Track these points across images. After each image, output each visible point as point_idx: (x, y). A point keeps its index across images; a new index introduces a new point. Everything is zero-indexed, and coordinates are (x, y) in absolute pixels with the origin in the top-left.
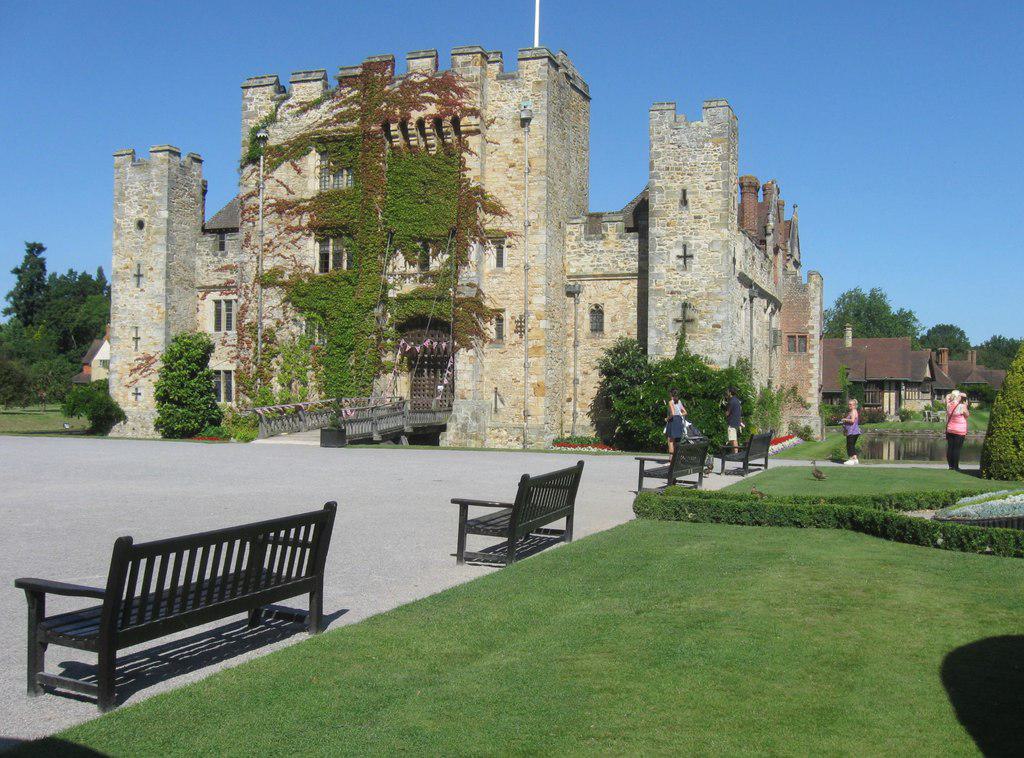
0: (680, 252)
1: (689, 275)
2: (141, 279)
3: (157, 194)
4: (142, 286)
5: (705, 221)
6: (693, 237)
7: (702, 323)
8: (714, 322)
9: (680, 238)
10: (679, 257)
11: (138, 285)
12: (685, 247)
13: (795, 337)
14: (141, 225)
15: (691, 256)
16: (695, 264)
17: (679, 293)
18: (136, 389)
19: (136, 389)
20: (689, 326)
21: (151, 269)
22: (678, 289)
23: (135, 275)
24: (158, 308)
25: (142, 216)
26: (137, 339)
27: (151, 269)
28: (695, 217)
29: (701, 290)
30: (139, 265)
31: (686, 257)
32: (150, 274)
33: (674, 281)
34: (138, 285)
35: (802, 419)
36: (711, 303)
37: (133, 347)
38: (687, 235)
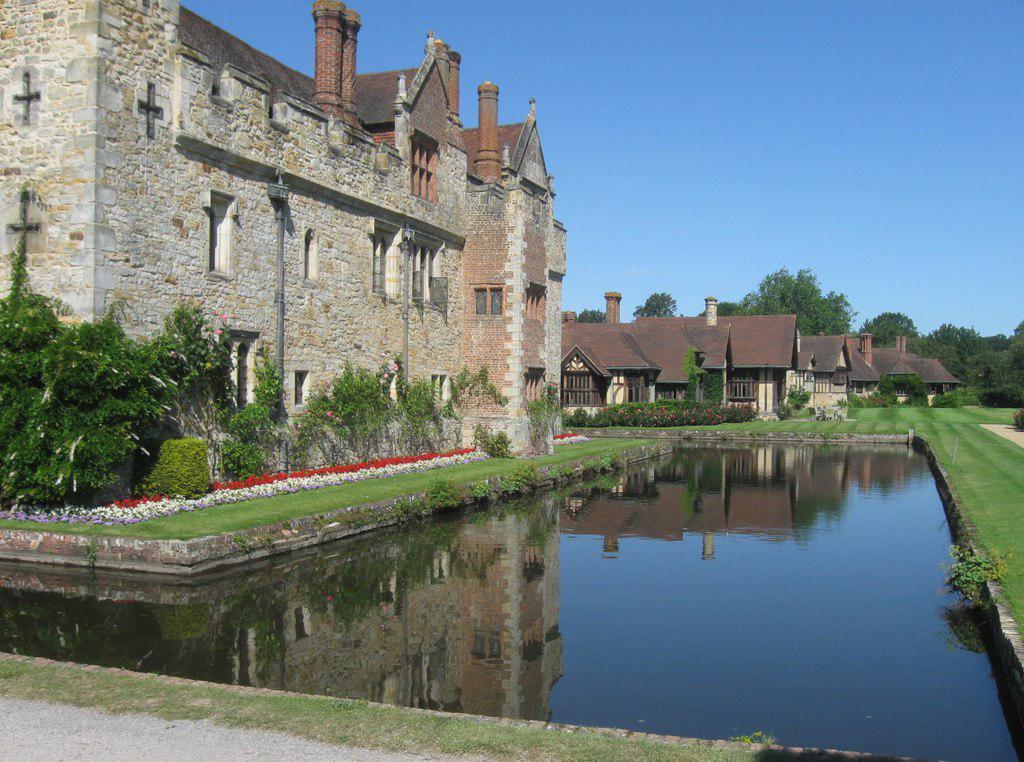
0: (18, 88)
1: (33, 135)
5: (61, 23)
6: (42, 56)
7: (53, 231)
8: (73, 229)
9: (21, 60)
10: (18, 98)
12: (27, 75)
13: (484, 290)
15: (37, 96)
16: (44, 108)
17: (18, 172)
20: (32, 239)
22: (16, 164)
28: (46, 16)
29: (54, 164)
31: (30, 98)
33: (9, 148)
35: (494, 423)
36: (68, 189)
38: (32, 52)
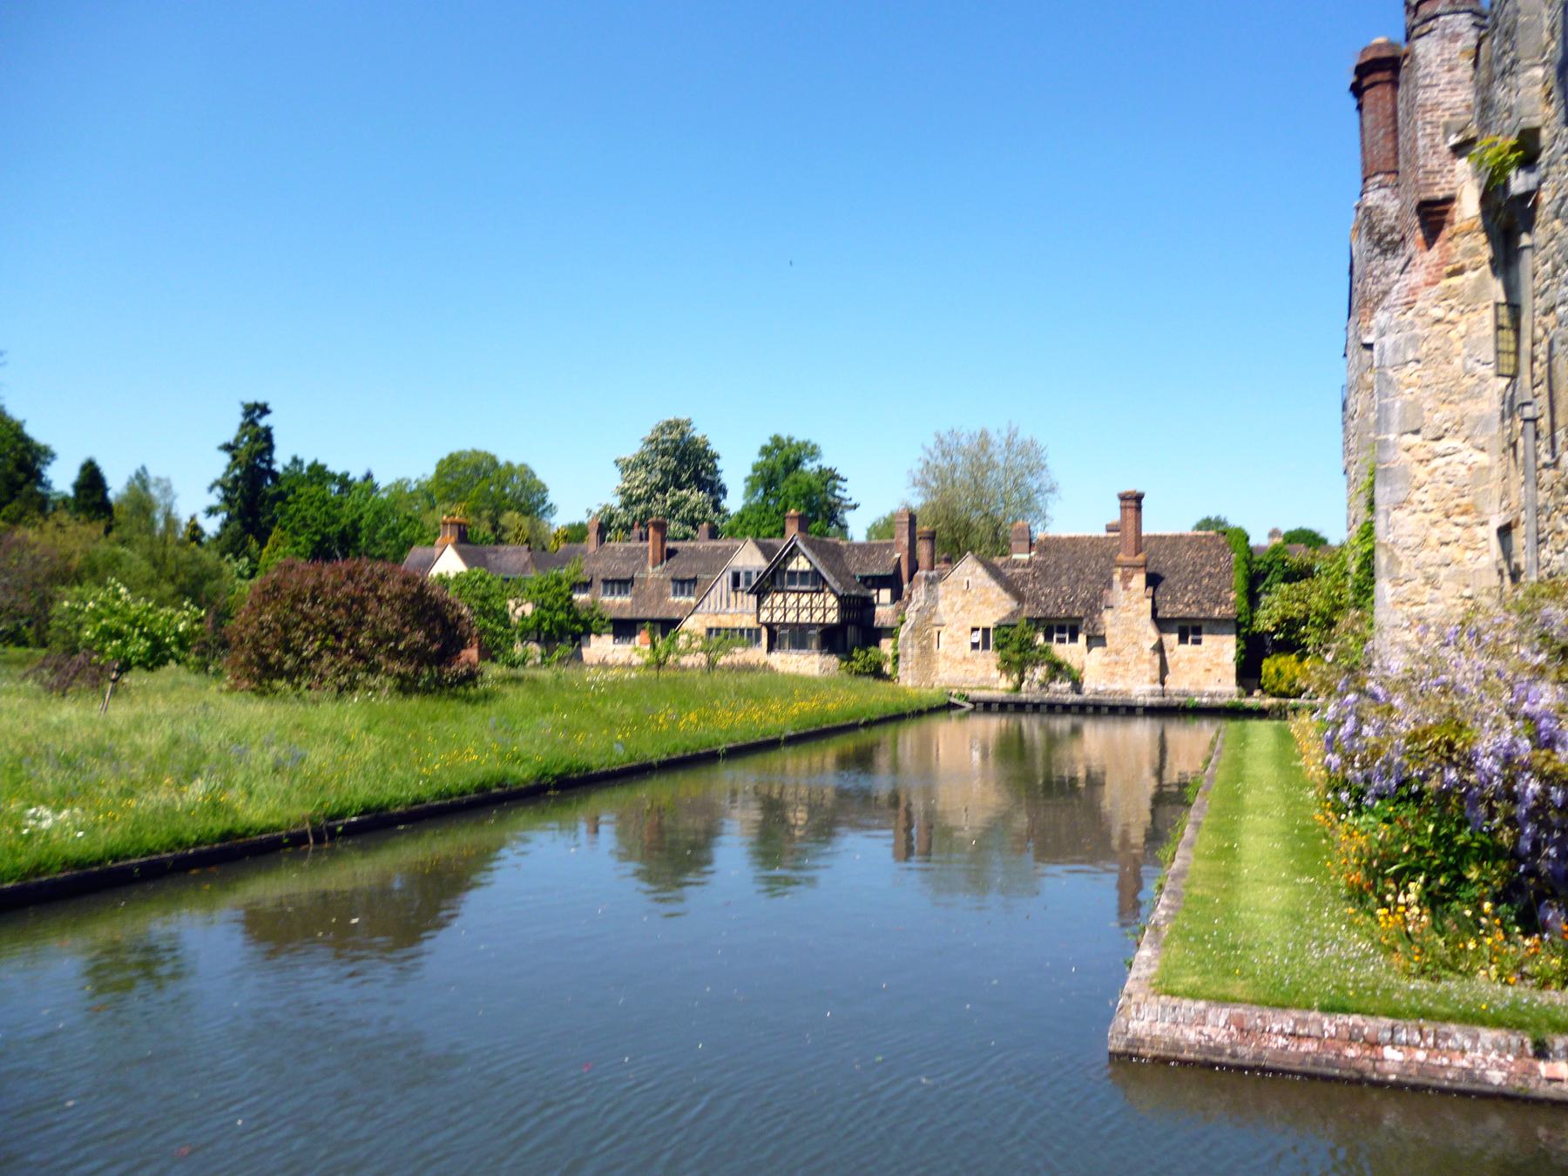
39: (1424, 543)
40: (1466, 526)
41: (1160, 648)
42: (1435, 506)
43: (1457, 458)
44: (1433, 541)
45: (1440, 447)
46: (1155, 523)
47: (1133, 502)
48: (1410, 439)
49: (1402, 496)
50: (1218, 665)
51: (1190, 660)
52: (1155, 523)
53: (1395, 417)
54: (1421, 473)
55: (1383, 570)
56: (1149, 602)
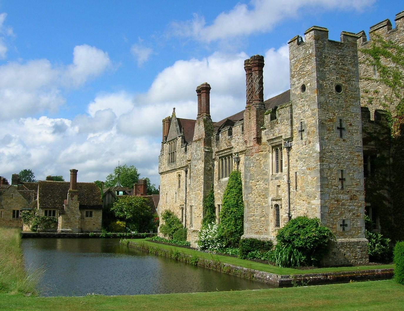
2: (343, 131)
3: (350, 67)
4: (345, 137)
11: (341, 136)
14: (338, 88)
18: (344, 221)
19: (344, 221)
21: (351, 125)
23: (338, 128)
24: (358, 156)
25: (340, 82)
26: (342, 180)
27: (351, 125)
30: (341, 120)
32: (351, 128)
34: (341, 136)
37: (340, 187)
39: (254, 201)
40: (263, 198)
41: (82, 218)
42: (257, 194)
43: (261, 186)
44: (256, 201)
45: (258, 183)
46: (79, 180)
47: (74, 173)
48: (251, 181)
49: (250, 192)
50: (97, 223)
51: (89, 222)
52: (79, 180)
53: (248, 177)
54: (254, 188)
55: (246, 206)
56: (78, 204)
